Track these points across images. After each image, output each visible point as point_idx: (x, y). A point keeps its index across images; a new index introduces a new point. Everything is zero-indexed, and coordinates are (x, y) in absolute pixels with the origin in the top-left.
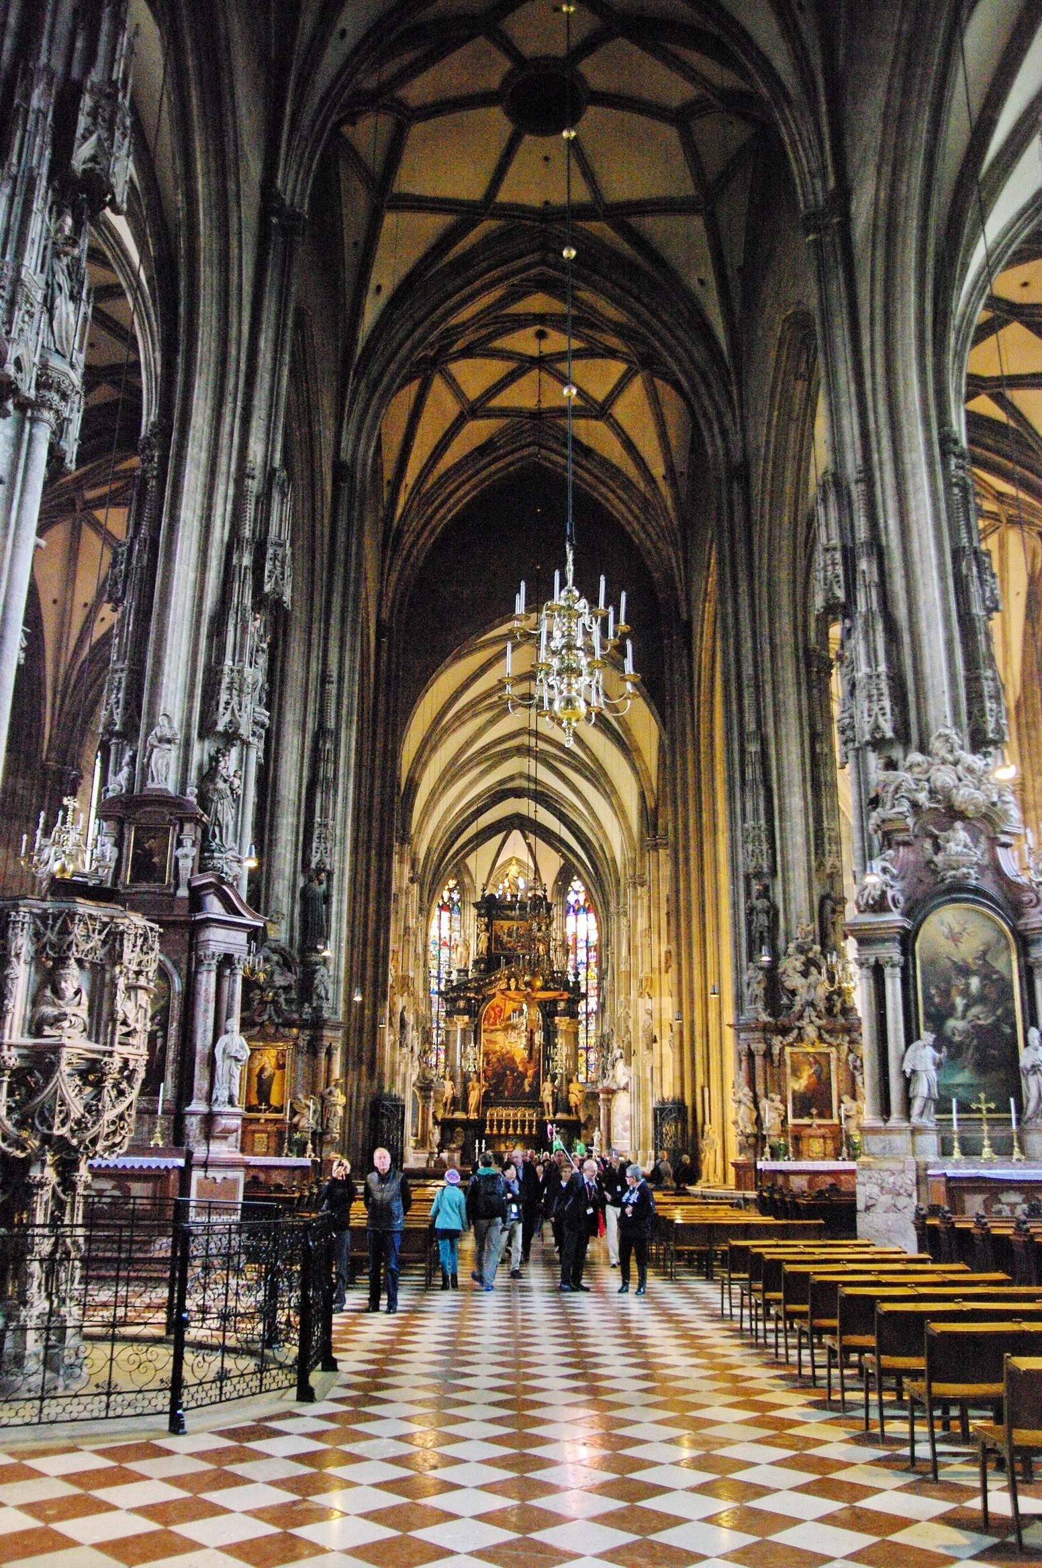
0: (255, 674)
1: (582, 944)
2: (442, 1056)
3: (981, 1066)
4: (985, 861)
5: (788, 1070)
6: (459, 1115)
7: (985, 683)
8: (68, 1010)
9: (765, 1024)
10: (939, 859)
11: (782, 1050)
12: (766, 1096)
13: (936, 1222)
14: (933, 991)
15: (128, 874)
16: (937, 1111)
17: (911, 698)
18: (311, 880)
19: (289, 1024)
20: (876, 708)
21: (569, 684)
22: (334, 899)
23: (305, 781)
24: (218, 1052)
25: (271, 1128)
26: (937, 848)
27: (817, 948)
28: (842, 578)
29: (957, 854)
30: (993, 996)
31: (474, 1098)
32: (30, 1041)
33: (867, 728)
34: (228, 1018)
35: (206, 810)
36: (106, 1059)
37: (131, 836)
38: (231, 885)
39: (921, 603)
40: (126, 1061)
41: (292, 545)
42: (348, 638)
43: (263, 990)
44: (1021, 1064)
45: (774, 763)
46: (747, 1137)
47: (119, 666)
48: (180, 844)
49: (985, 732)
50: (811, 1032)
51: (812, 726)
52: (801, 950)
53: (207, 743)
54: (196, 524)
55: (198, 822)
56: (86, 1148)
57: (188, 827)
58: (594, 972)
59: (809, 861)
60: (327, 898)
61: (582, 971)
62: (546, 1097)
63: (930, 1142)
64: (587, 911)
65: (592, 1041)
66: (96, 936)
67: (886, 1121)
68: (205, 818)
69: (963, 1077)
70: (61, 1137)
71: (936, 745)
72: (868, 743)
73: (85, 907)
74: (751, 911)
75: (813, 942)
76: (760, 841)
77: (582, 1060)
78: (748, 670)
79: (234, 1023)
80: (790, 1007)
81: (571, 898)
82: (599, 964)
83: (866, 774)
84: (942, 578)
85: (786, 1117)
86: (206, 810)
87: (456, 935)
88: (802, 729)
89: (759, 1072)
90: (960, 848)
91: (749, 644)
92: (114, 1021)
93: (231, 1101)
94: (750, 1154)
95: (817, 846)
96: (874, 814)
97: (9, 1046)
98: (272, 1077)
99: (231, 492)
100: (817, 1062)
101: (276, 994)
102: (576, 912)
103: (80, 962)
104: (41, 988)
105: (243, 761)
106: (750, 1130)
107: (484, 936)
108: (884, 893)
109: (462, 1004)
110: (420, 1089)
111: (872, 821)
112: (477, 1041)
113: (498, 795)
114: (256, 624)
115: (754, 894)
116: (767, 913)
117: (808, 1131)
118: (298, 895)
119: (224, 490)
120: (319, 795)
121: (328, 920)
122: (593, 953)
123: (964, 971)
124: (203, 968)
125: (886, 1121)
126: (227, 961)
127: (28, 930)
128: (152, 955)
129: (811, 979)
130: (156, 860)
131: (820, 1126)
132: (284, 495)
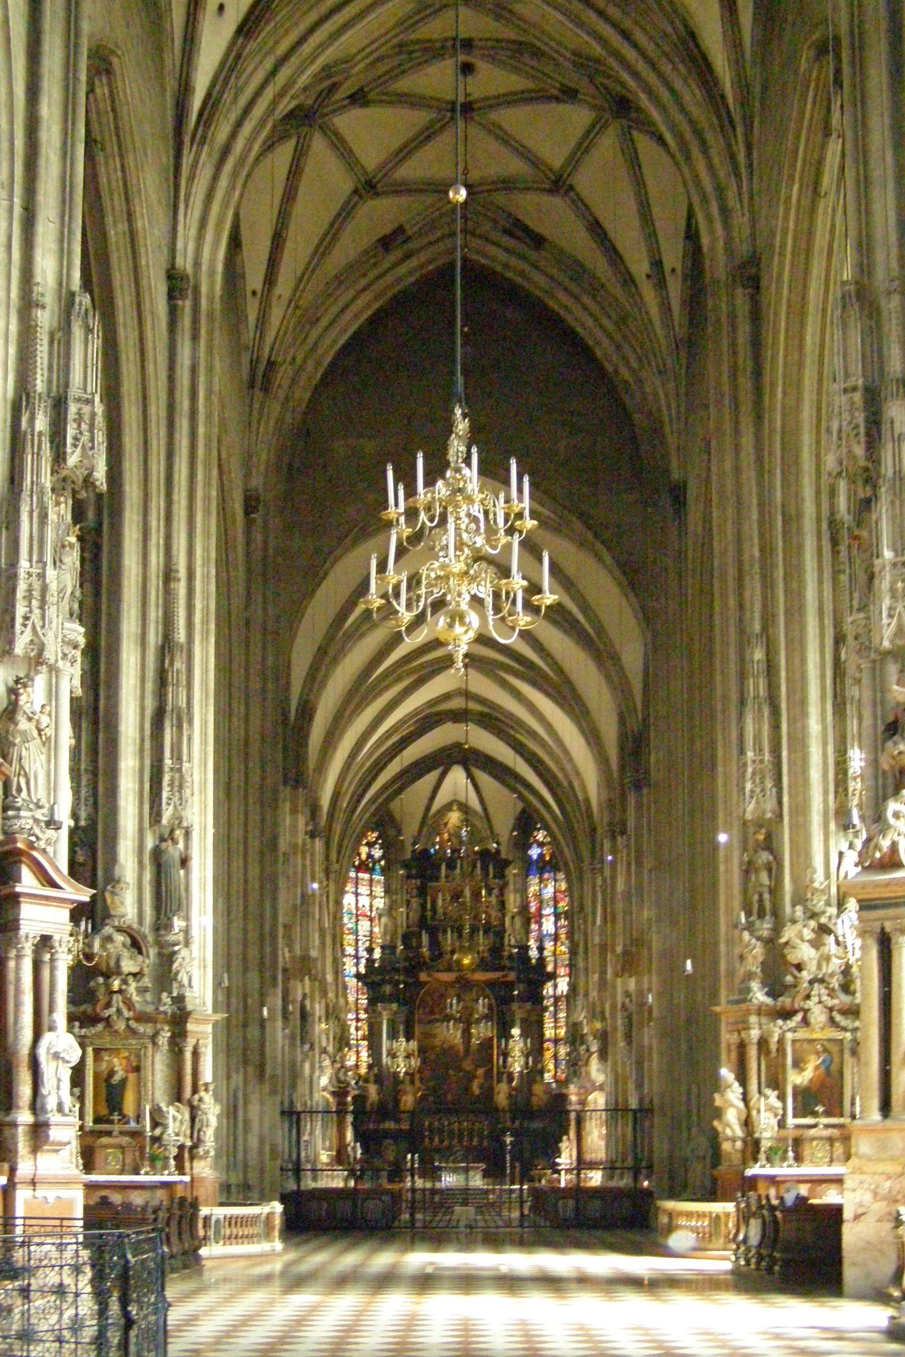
1: (548, 911)
19: (142, 1018)
24: (42, 1052)
34: (51, 1011)
43: (107, 976)
50: (818, 1016)
61: (549, 945)
82: (570, 935)
87: (380, 903)
98: (124, 1081)
100: (825, 1050)
101: (125, 982)
107: (415, 903)
117: (812, 1132)
122: (563, 922)
126: (45, 942)
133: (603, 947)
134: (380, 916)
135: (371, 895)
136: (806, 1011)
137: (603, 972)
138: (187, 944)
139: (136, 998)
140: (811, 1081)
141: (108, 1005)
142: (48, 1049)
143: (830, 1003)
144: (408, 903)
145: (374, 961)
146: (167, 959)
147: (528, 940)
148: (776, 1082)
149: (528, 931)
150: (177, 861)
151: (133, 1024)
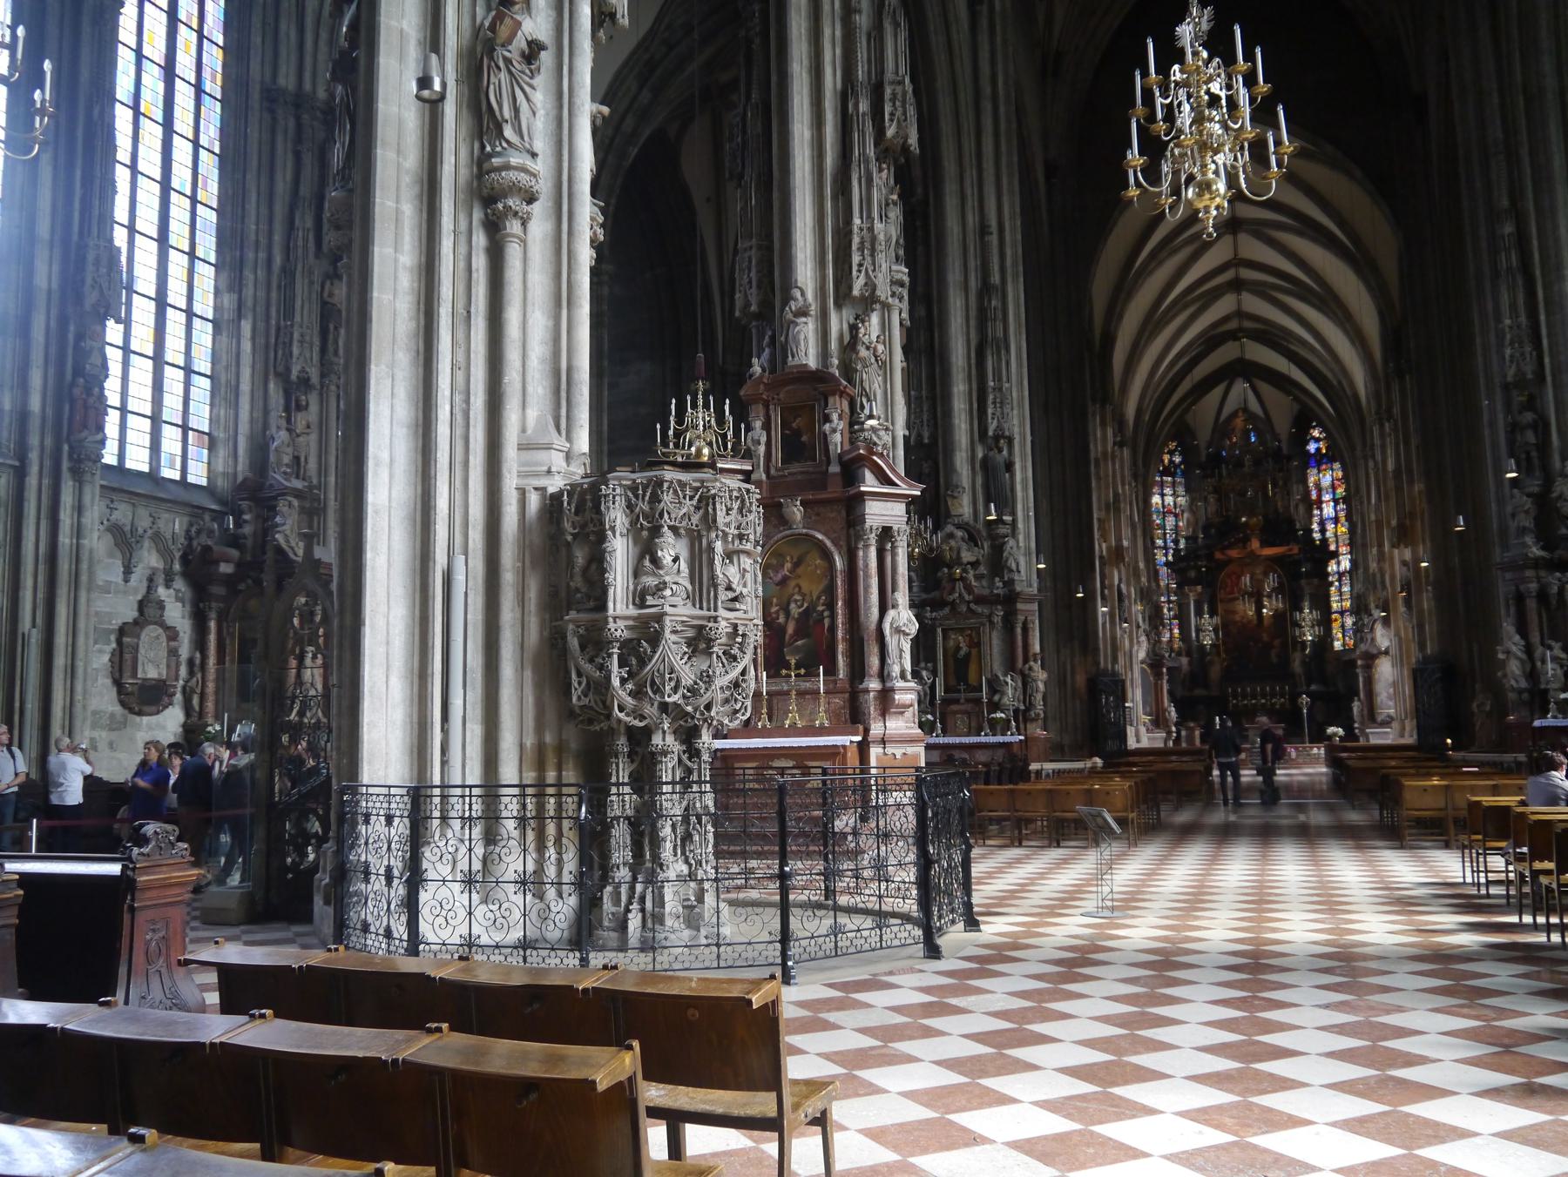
0: (888, 229)
1: (1327, 497)
2: (1176, 631)
6: (1199, 692)
8: (667, 579)
12: (1543, 644)
15: (777, 455)
19: (980, 600)
21: (1204, 166)
22: (1018, 466)
25: (969, 707)
31: (1215, 672)
32: (632, 611)
34: (893, 592)
35: (850, 381)
36: (710, 625)
37: (777, 420)
38: (881, 456)
40: (735, 627)
41: (912, 80)
42: (1005, 181)
43: (950, 567)
45: (1535, 243)
47: (747, 244)
48: (827, 419)
53: (844, 312)
54: (805, 76)
55: (842, 394)
56: (703, 714)
57: (831, 400)
58: (1342, 529)
60: (1009, 466)
61: (1330, 527)
62: (1297, 666)
65: (1347, 604)
66: (688, 502)
68: (850, 390)
70: (675, 703)
73: (670, 474)
74: (1514, 428)
76: (1521, 343)
77: (1336, 626)
79: (902, 597)
81: (1312, 447)
82: (1349, 518)
86: (850, 381)
92: (715, 586)
93: (903, 676)
97: (615, 618)
98: (968, 655)
99: (838, 33)
101: (964, 571)
102: (1318, 465)
103: (674, 529)
104: (641, 558)
105: (885, 326)
106: (1523, 684)
107: (1211, 499)
109: (1192, 574)
110: (1151, 666)
112: (1212, 613)
113: (1212, 340)
114: (883, 178)
116: (1534, 426)
118: (978, 466)
119: (831, 32)
120: (990, 358)
121: (1013, 489)
124: (860, 546)
126: (886, 533)
127: (620, 502)
128: (751, 517)
130: (804, 438)
132: (896, 25)
133: (1379, 524)
134: (1183, 511)
135: (1175, 495)
137: (1380, 545)
138: (1014, 534)
139: (974, 583)
141: (952, 590)
142: (891, 624)
144: (1206, 498)
145: (1180, 550)
146: (998, 549)
147: (1311, 524)
149: (1311, 516)
150: (1003, 469)
151: (972, 605)
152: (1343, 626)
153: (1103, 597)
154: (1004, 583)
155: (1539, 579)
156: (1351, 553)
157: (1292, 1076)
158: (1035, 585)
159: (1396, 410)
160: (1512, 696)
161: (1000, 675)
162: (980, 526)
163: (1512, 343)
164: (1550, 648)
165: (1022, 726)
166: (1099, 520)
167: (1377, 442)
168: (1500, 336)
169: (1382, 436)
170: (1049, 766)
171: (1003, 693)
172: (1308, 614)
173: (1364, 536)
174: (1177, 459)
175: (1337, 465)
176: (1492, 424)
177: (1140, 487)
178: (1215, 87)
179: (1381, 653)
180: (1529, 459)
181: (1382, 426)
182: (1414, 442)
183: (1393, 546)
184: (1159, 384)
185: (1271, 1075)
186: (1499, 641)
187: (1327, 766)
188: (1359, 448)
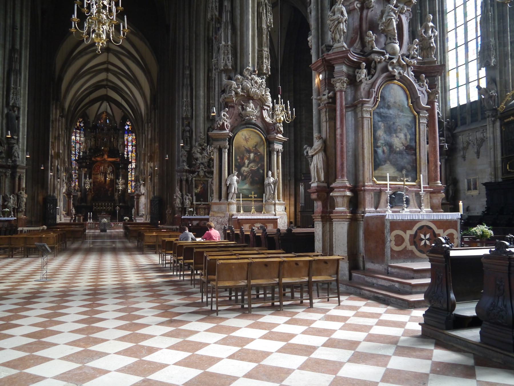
1: (130, 144)
2: (77, 183)
3: (252, 183)
4: (259, 114)
5: (194, 186)
6: (83, 204)
7: (264, 52)
9: (186, 170)
10: (243, 113)
11: (192, 179)
13: (229, 231)
14: (238, 158)
16: (236, 198)
17: (239, 55)
18: (10, 110)
20: (226, 58)
21: (99, 28)
22: (21, 119)
23: (6, 70)
26: (243, 109)
27: (206, 144)
28: (218, 8)
29: (249, 111)
30: (257, 160)
31: (89, 198)
33: (222, 65)
39: (245, 21)
44: (265, 183)
45: (194, 78)
46: (179, 208)
49: (263, 70)
50: (202, 173)
51: (209, 66)
52: (200, 145)
58: (134, 155)
59: (204, 114)
60: (18, 118)
61: (130, 154)
62: (116, 197)
63: (234, 208)
64: (132, 133)
67: (220, 200)
69: (246, 186)
71: (246, 73)
72: (222, 70)
74: (184, 131)
75: (205, 142)
76: (188, 106)
77: (129, 185)
78: (187, 43)
80: (195, 165)
81: (127, 127)
82: (136, 151)
83: (221, 81)
84: (253, 12)
85: (193, 201)
88: (205, 67)
89: (184, 187)
90: (250, 110)
91: (188, 34)
94: (180, 214)
95: (207, 108)
96: (223, 95)
100: (203, 183)
102: (128, 133)
106: (180, 206)
107: (93, 140)
108: (223, 123)
109: (84, 164)
110: (67, 194)
111: (222, 98)
113: (97, 87)
115: (185, 125)
116: (189, 131)
117: (200, 206)
118: (4, 116)
122: (134, 147)
123: (249, 151)
125: (220, 200)
129: (203, 155)
131: (204, 204)
134: (82, 143)
135: (80, 137)
136: (198, 172)
137: (144, 161)
140: (200, 191)
143: (205, 170)
144: (91, 140)
145: (80, 156)
148: (190, 191)
149: (124, 149)
152: (131, 185)
153: (51, 169)
154: (12, 161)
155: (186, 175)
156: (136, 163)
157: (104, 327)
158: (25, 163)
159: (153, 120)
160: (177, 209)
161: (8, 195)
162: (4, 139)
163: (185, 106)
164: (188, 196)
165: (16, 214)
166: (52, 142)
167: (146, 129)
168: (183, 102)
169: (148, 128)
170: (26, 229)
171: (9, 202)
172: (121, 181)
173: (140, 158)
174: (82, 125)
175: (134, 134)
176: (178, 129)
177: (68, 133)
178: (105, 3)
179: (142, 194)
180: (187, 141)
181: (148, 124)
182: (157, 130)
183: (148, 162)
184: (77, 98)
185: (97, 327)
186: (175, 193)
187: (123, 229)
188: (141, 130)
